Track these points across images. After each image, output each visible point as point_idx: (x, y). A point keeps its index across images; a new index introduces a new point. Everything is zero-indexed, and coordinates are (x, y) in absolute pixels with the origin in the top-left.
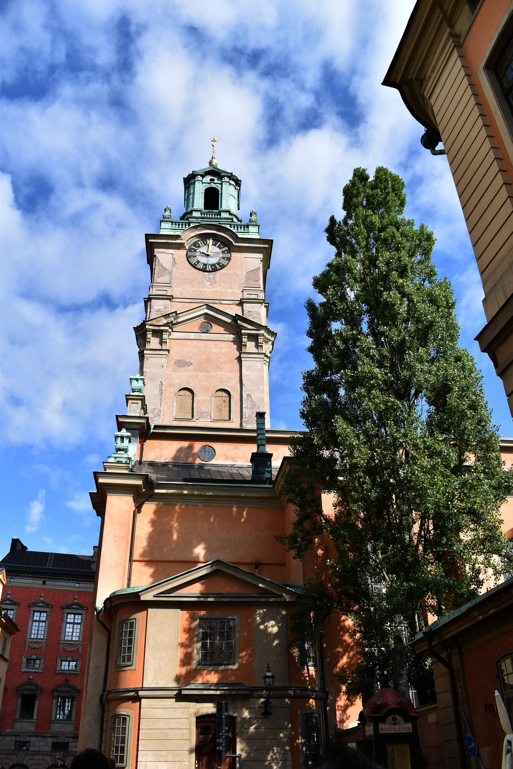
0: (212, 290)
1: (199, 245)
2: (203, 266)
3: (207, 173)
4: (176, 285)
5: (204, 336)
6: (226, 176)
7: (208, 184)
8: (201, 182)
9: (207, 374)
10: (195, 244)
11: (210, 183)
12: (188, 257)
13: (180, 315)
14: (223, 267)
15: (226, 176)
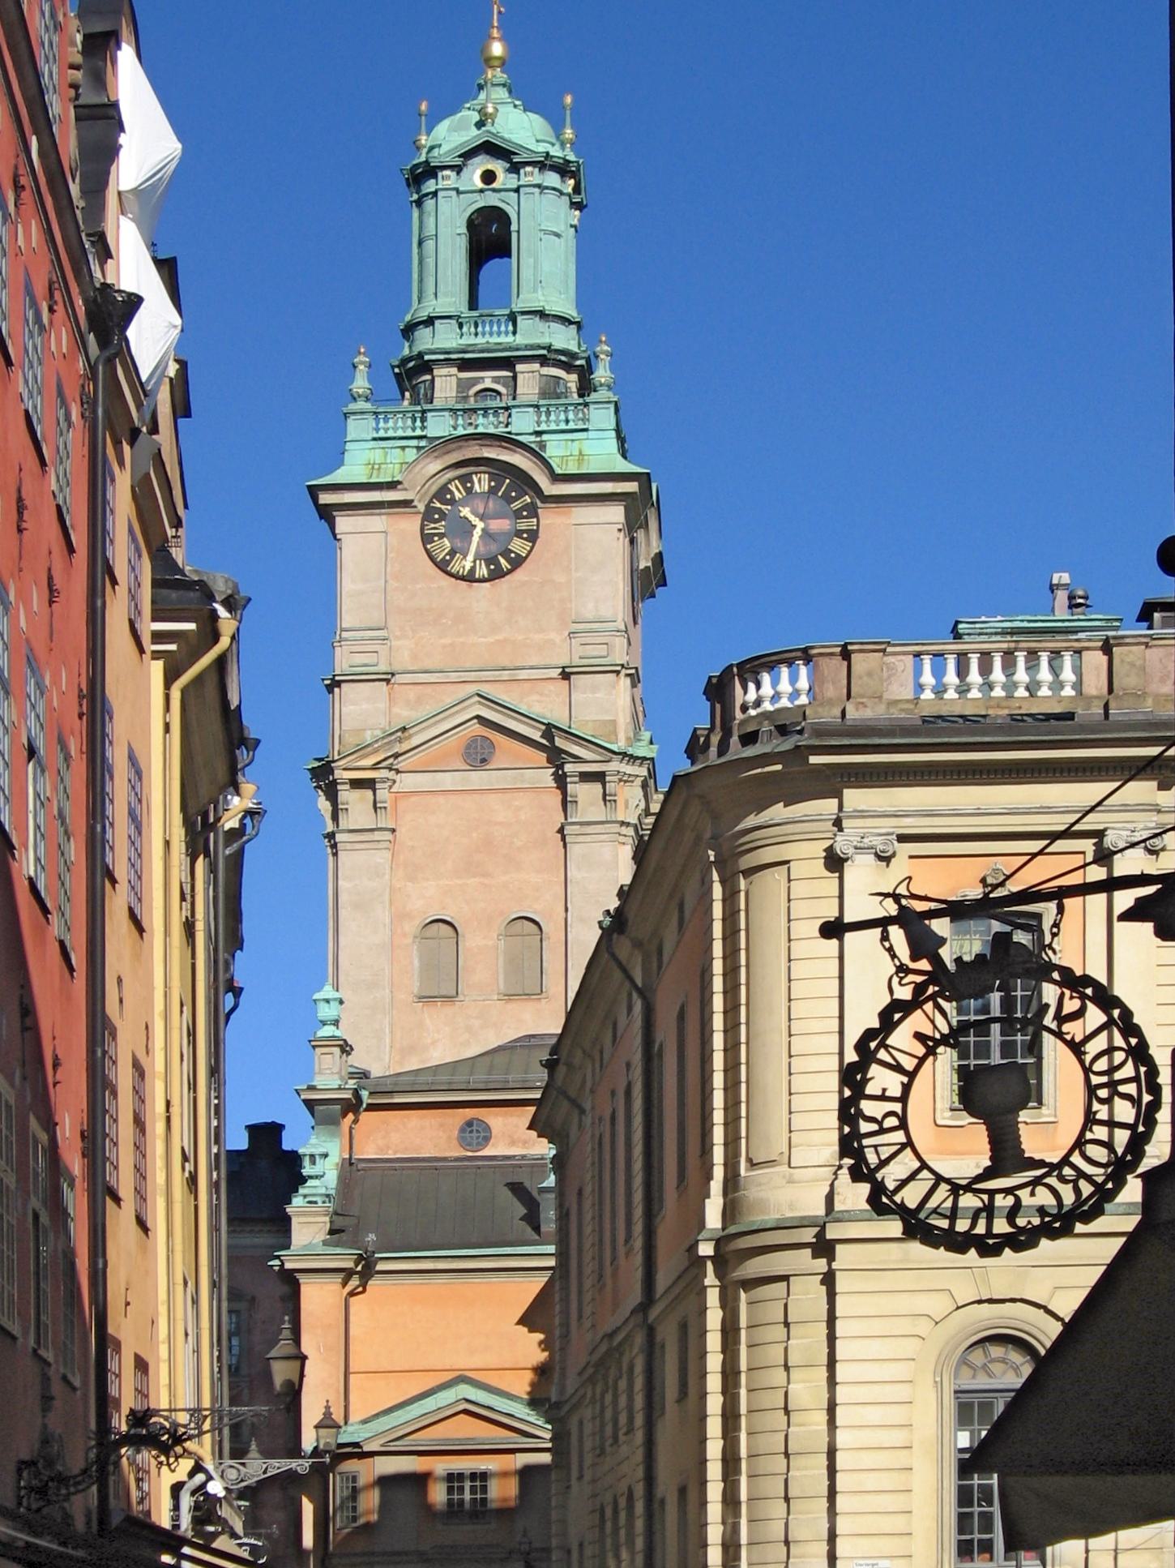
0: (491, 639)
4: (398, 633)
5: (478, 779)
9: (486, 881)
10: (444, 489)
11: (482, 191)
12: (426, 539)
13: (411, 731)
14: (517, 562)
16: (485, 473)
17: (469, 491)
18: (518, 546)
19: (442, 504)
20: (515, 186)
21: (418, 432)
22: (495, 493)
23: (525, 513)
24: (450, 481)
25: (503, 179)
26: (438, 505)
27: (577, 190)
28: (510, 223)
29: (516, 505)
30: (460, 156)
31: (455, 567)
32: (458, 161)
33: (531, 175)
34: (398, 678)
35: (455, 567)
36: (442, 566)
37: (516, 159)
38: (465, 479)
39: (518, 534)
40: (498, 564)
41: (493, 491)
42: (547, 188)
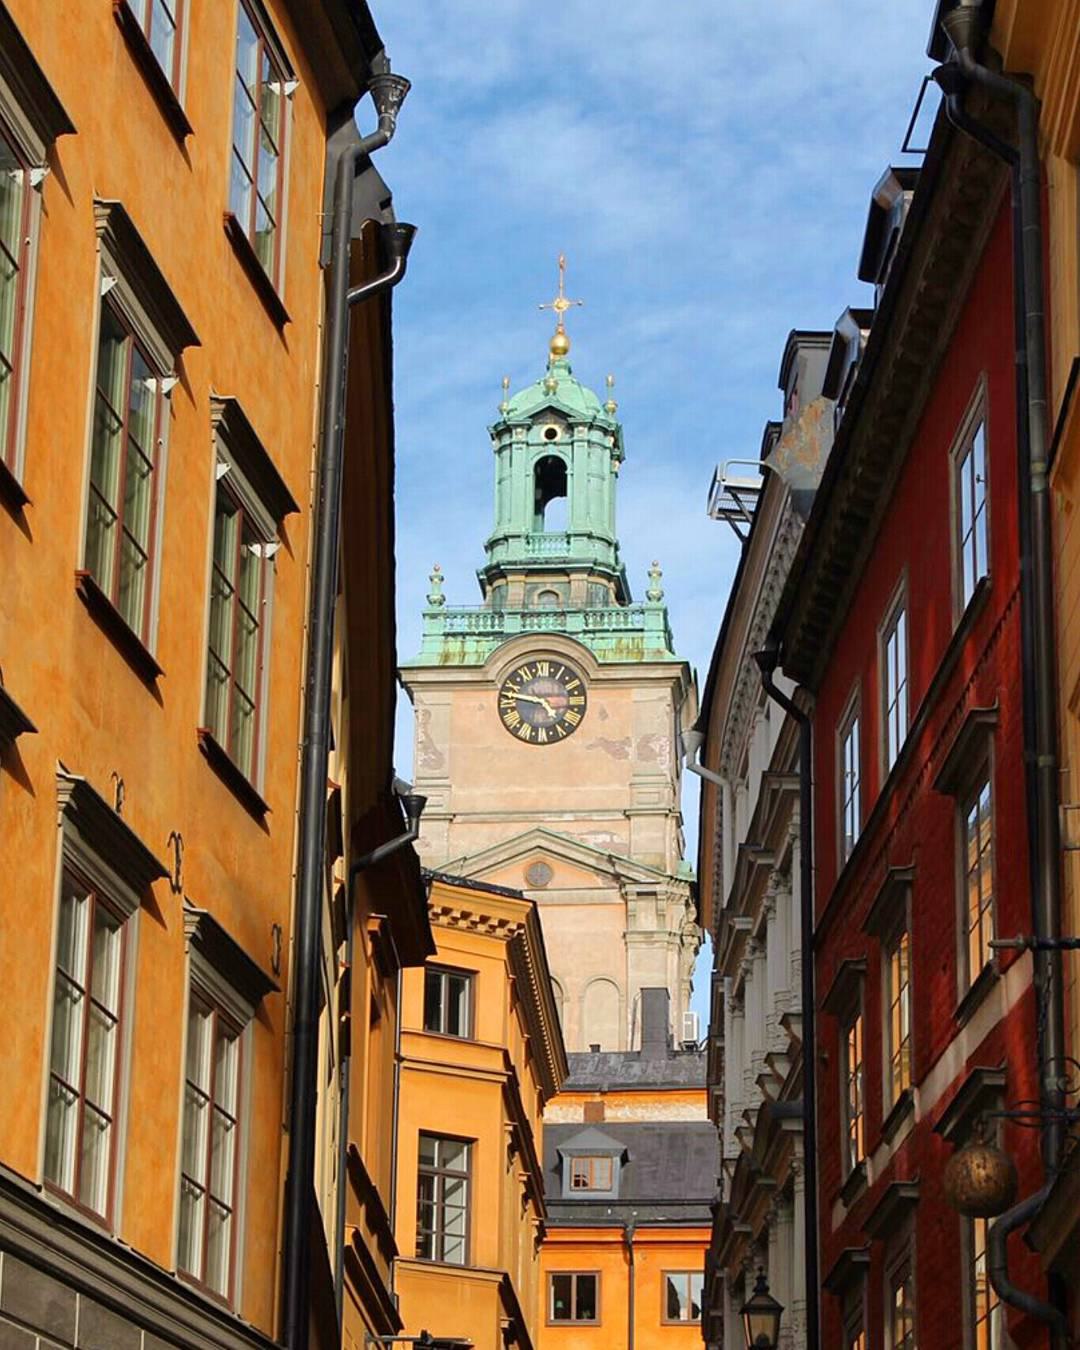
1: (522, 677)
2: (532, 731)
3: (537, 417)
6: (581, 424)
7: (541, 448)
8: (524, 446)
11: (546, 444)
14: (571, 730)
15: (581, 424)
16: (545, 661)
17: (534, 675)
18: (570, 717)
19: (514, 684)
20: (570, 441)
21: (497, 629)
22: (554, 677)
23: (576, 693)
24: (520, 668)
25: (561, 436)
26: (511, 685)
27: (616, 445)
28: (565, 468)
29: (569, 687)
30: (530, 417)
31: (521, 733)
32: (529, 422)
33: (581, 433)
35: (521, 733)
36: (514, 732)
37: (571, 420)
39: (571, 708)
40: (556, 731)
41: (552, 675)
42: (594, 443)
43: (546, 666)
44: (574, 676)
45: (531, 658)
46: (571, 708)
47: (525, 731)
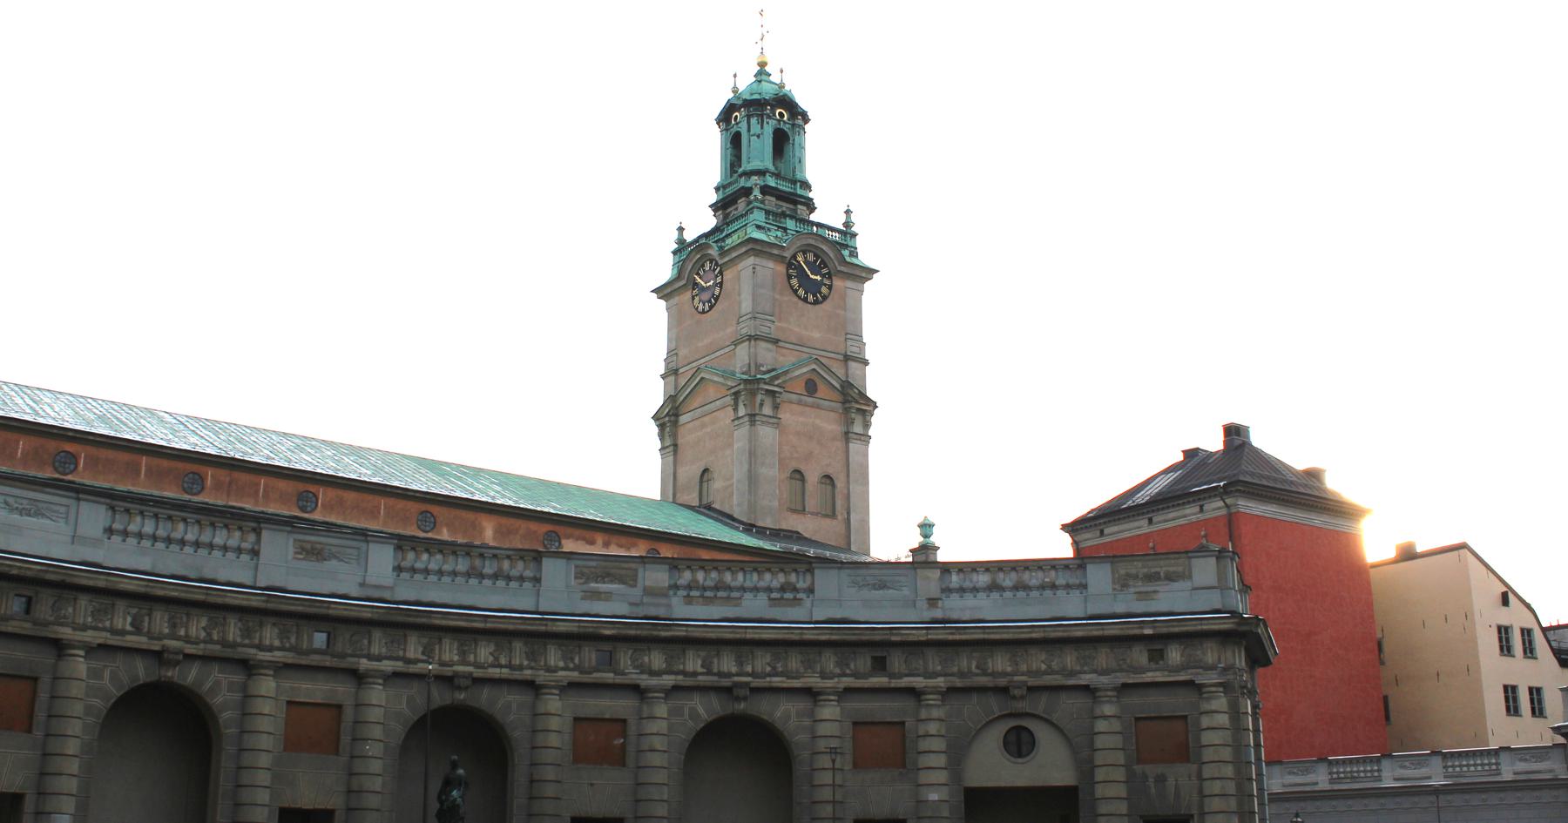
12: (789, 277)
14: (825, 298)
34: (781, 344)
36: (795, 292)
38: (804, 253)
39: (825, 285)
40: (817, 298)
41: (815, 261)
43: (812, 254)
44: (826, 266)
45: (803, 248)
46: (825, 285)
47: (801, 292)
